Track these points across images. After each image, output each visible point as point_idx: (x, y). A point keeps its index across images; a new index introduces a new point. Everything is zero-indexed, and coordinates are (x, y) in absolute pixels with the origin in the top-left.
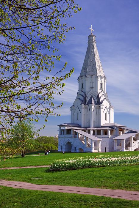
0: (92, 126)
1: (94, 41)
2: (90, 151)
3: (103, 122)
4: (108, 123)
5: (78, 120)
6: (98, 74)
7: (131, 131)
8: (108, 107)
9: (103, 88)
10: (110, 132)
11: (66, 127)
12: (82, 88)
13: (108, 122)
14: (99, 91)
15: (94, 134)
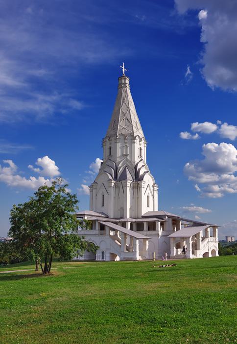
0: (128, 216)
1: (127, 85)
2: (132, 258)
3: (145, 210)
4: (152, 211)
5: (103, 206)
6: (135, 135)
7: (194, 223)
8: (151, 185)
9: (143, 155)
10: (159, 223)
11: (86, 218)
12: (110, 155)
13: (151, 209)
14: (137, 160)
15: (131, 229)
